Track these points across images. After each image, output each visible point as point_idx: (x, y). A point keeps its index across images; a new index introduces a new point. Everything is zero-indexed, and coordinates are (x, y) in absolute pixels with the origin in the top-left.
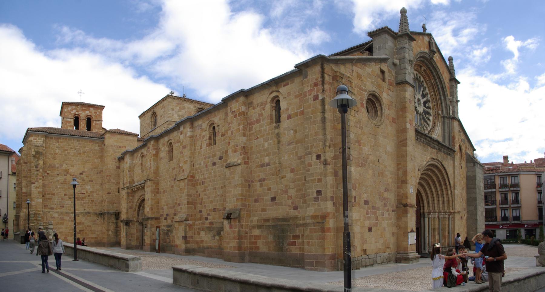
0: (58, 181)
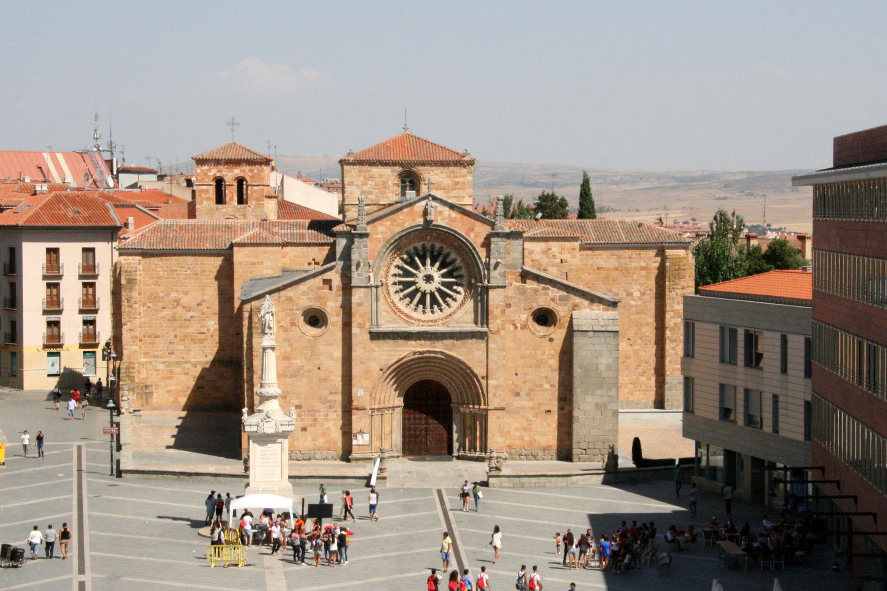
0: (164, 317)
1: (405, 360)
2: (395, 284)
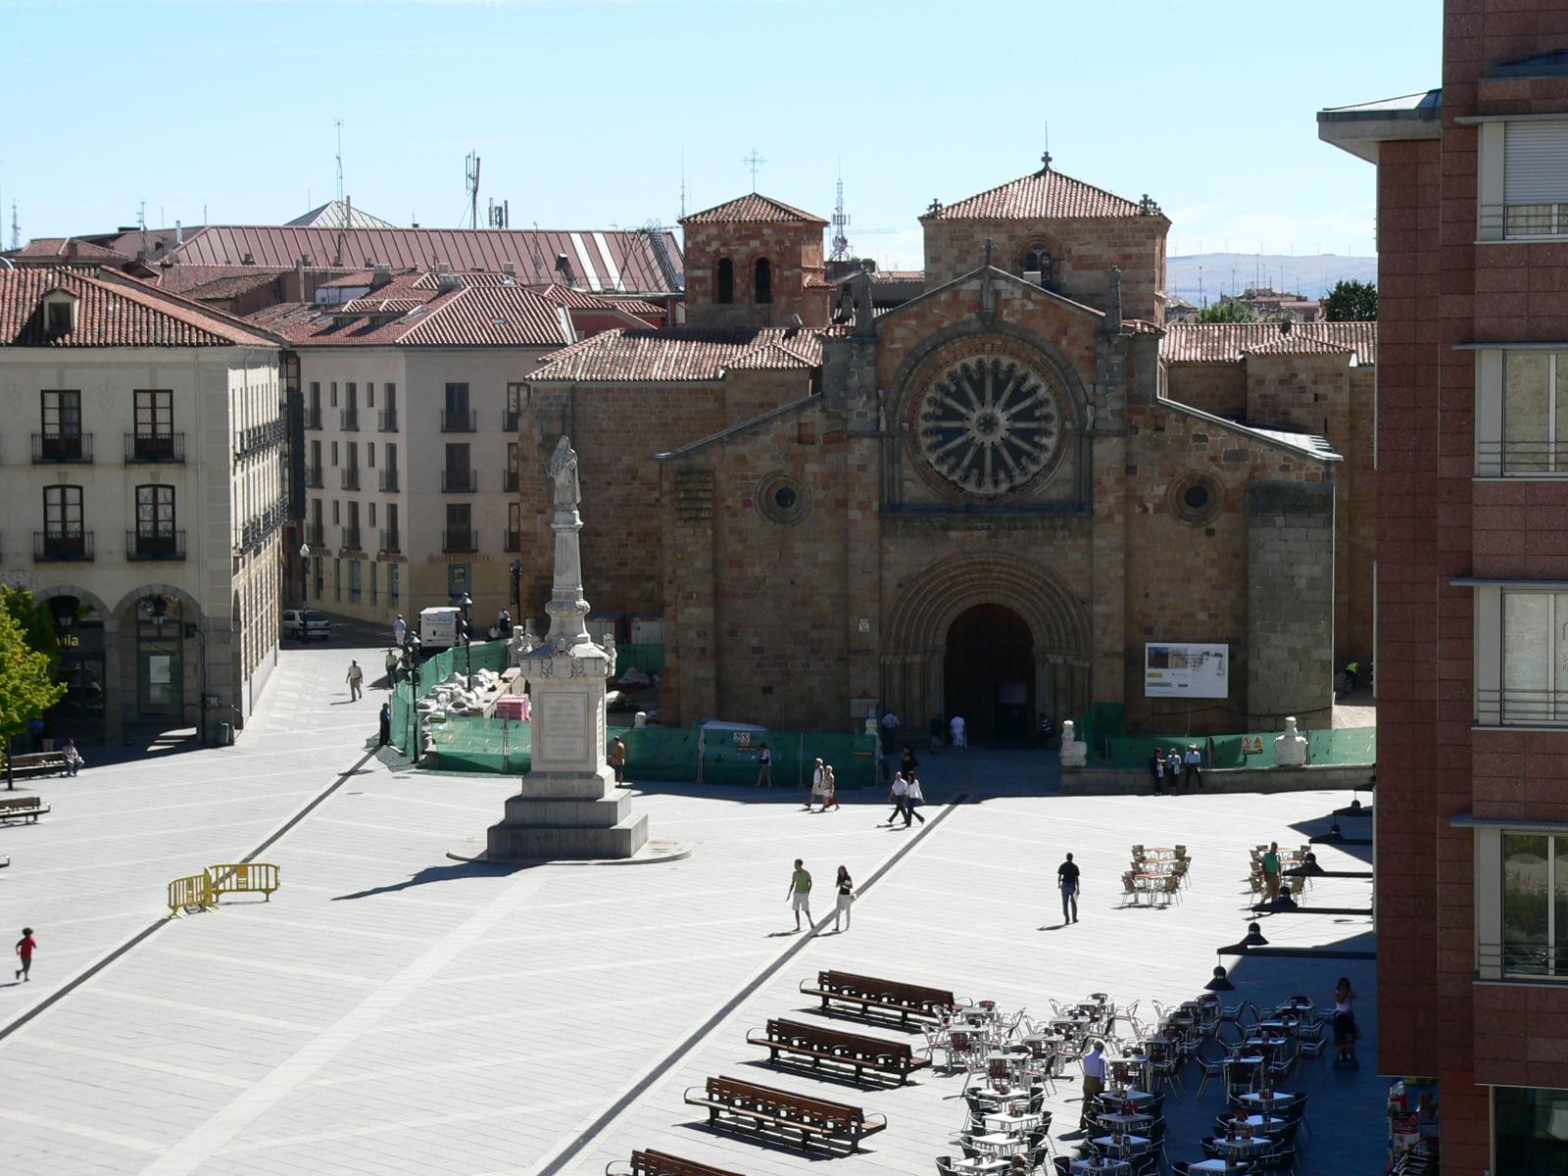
0: (611, 500)
2: (928, 433)
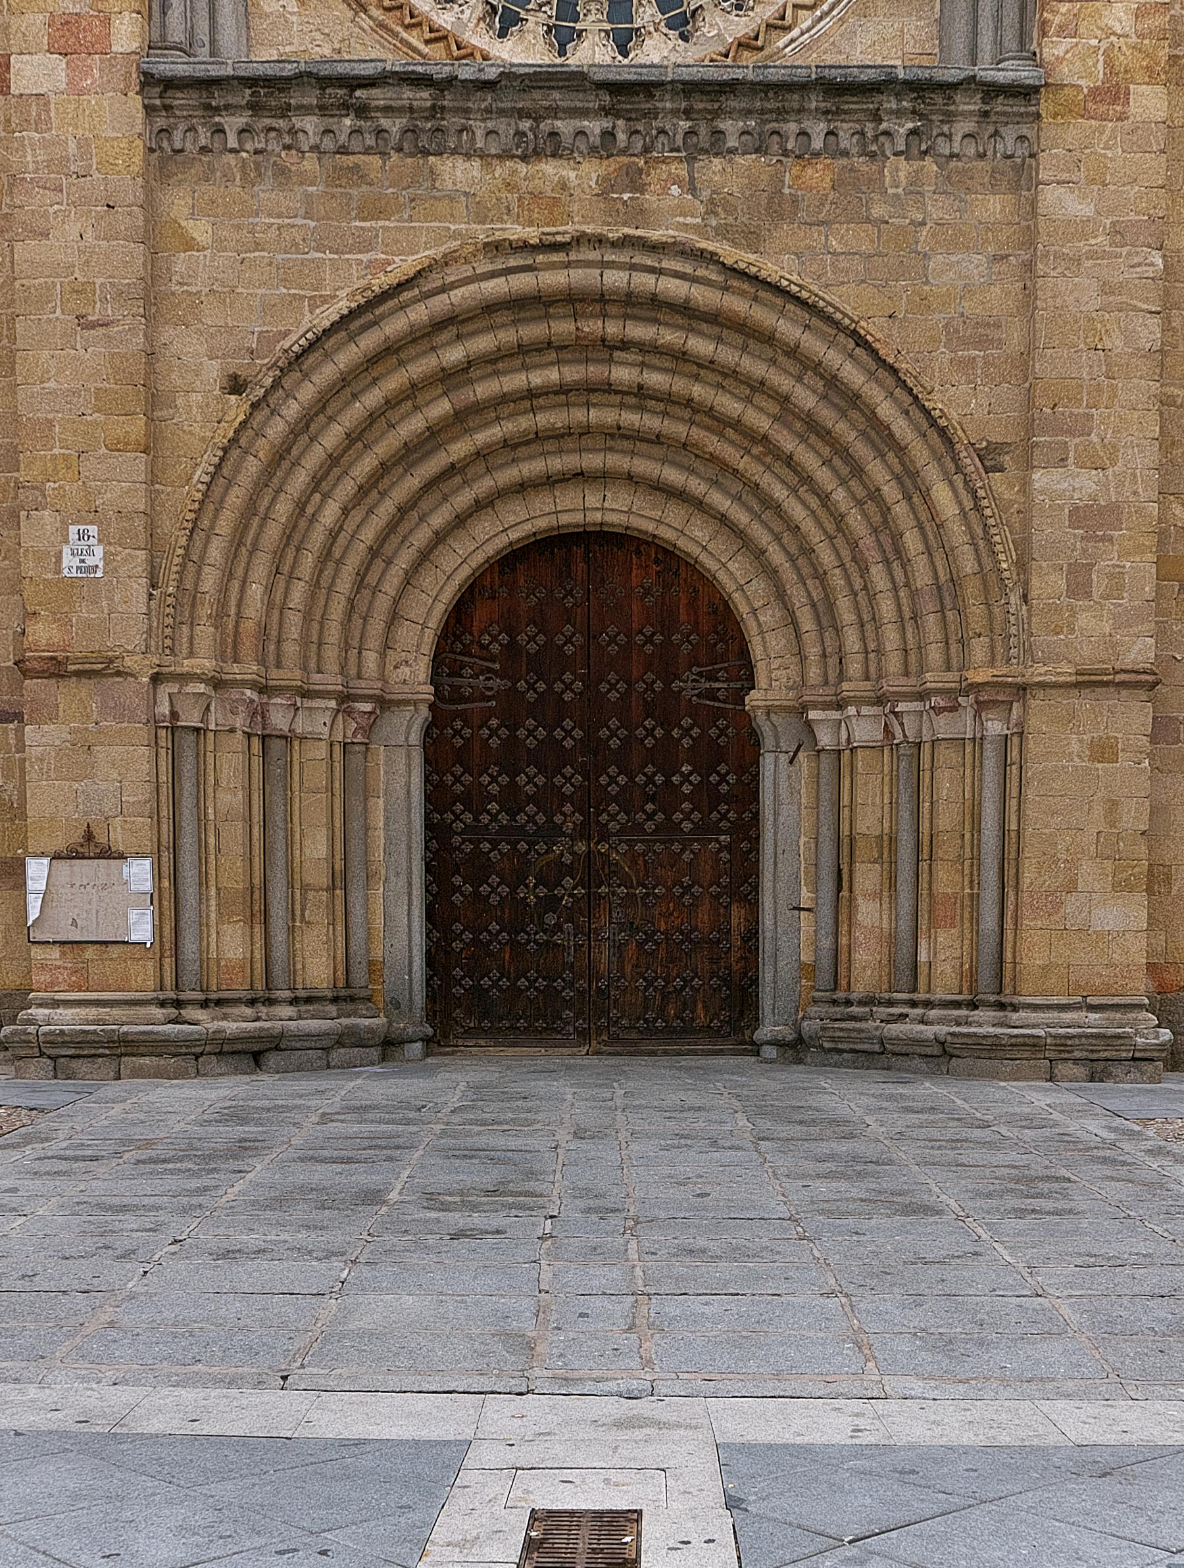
1: (419, 314)
